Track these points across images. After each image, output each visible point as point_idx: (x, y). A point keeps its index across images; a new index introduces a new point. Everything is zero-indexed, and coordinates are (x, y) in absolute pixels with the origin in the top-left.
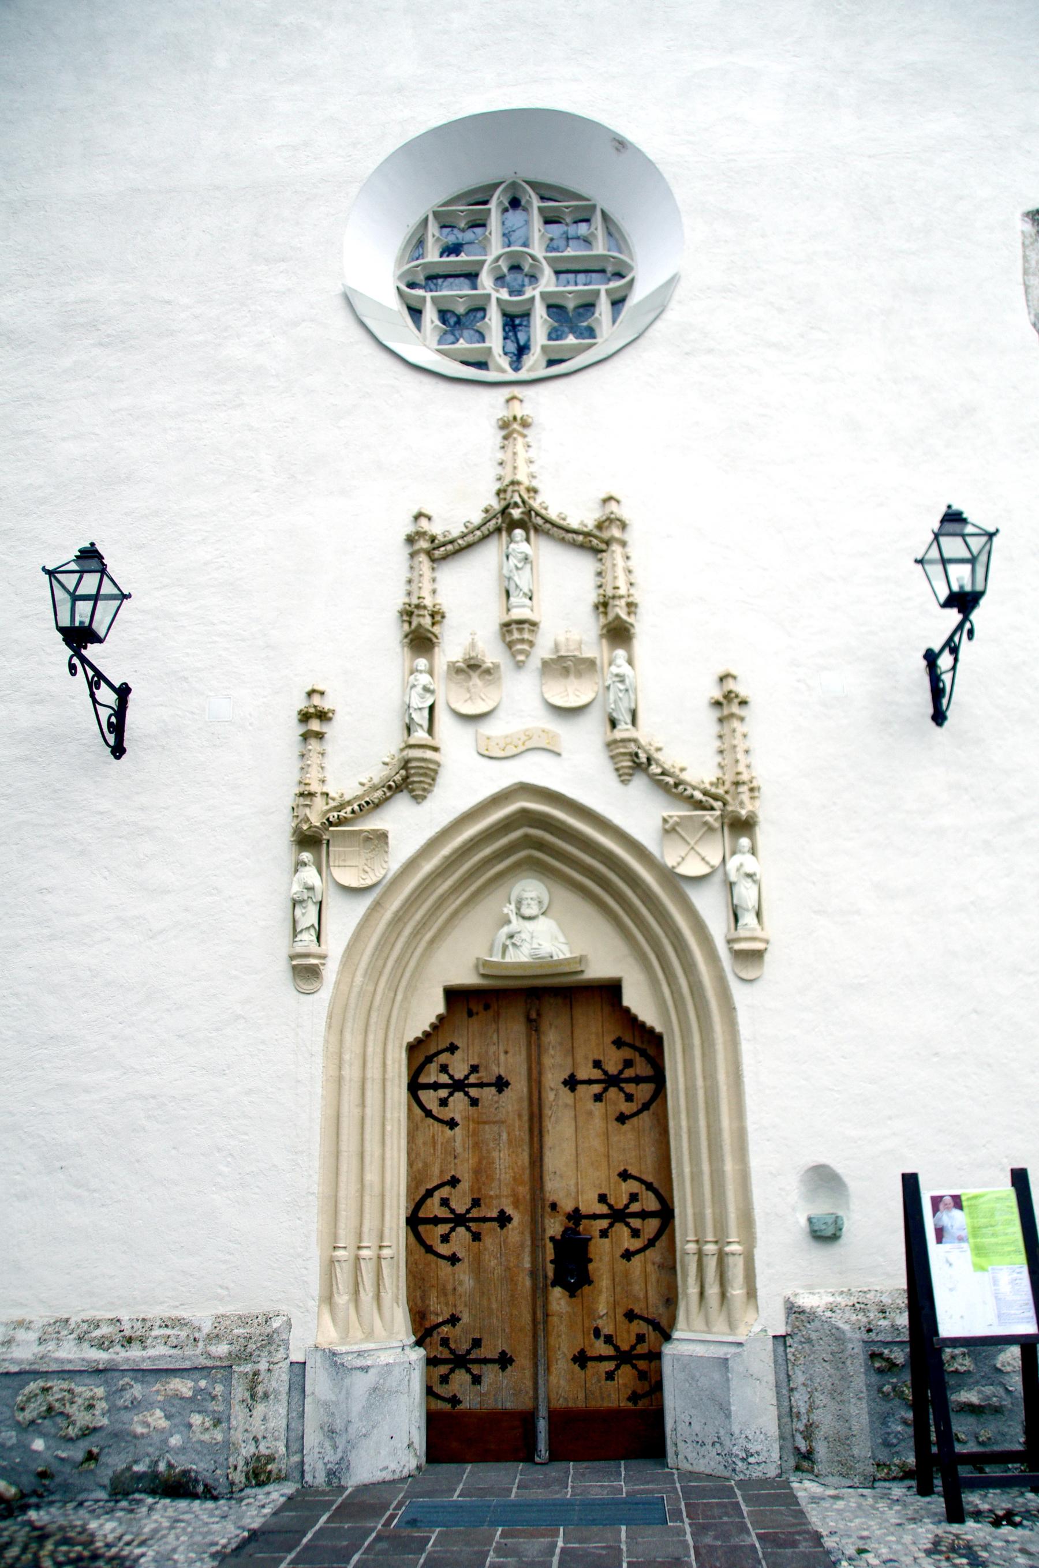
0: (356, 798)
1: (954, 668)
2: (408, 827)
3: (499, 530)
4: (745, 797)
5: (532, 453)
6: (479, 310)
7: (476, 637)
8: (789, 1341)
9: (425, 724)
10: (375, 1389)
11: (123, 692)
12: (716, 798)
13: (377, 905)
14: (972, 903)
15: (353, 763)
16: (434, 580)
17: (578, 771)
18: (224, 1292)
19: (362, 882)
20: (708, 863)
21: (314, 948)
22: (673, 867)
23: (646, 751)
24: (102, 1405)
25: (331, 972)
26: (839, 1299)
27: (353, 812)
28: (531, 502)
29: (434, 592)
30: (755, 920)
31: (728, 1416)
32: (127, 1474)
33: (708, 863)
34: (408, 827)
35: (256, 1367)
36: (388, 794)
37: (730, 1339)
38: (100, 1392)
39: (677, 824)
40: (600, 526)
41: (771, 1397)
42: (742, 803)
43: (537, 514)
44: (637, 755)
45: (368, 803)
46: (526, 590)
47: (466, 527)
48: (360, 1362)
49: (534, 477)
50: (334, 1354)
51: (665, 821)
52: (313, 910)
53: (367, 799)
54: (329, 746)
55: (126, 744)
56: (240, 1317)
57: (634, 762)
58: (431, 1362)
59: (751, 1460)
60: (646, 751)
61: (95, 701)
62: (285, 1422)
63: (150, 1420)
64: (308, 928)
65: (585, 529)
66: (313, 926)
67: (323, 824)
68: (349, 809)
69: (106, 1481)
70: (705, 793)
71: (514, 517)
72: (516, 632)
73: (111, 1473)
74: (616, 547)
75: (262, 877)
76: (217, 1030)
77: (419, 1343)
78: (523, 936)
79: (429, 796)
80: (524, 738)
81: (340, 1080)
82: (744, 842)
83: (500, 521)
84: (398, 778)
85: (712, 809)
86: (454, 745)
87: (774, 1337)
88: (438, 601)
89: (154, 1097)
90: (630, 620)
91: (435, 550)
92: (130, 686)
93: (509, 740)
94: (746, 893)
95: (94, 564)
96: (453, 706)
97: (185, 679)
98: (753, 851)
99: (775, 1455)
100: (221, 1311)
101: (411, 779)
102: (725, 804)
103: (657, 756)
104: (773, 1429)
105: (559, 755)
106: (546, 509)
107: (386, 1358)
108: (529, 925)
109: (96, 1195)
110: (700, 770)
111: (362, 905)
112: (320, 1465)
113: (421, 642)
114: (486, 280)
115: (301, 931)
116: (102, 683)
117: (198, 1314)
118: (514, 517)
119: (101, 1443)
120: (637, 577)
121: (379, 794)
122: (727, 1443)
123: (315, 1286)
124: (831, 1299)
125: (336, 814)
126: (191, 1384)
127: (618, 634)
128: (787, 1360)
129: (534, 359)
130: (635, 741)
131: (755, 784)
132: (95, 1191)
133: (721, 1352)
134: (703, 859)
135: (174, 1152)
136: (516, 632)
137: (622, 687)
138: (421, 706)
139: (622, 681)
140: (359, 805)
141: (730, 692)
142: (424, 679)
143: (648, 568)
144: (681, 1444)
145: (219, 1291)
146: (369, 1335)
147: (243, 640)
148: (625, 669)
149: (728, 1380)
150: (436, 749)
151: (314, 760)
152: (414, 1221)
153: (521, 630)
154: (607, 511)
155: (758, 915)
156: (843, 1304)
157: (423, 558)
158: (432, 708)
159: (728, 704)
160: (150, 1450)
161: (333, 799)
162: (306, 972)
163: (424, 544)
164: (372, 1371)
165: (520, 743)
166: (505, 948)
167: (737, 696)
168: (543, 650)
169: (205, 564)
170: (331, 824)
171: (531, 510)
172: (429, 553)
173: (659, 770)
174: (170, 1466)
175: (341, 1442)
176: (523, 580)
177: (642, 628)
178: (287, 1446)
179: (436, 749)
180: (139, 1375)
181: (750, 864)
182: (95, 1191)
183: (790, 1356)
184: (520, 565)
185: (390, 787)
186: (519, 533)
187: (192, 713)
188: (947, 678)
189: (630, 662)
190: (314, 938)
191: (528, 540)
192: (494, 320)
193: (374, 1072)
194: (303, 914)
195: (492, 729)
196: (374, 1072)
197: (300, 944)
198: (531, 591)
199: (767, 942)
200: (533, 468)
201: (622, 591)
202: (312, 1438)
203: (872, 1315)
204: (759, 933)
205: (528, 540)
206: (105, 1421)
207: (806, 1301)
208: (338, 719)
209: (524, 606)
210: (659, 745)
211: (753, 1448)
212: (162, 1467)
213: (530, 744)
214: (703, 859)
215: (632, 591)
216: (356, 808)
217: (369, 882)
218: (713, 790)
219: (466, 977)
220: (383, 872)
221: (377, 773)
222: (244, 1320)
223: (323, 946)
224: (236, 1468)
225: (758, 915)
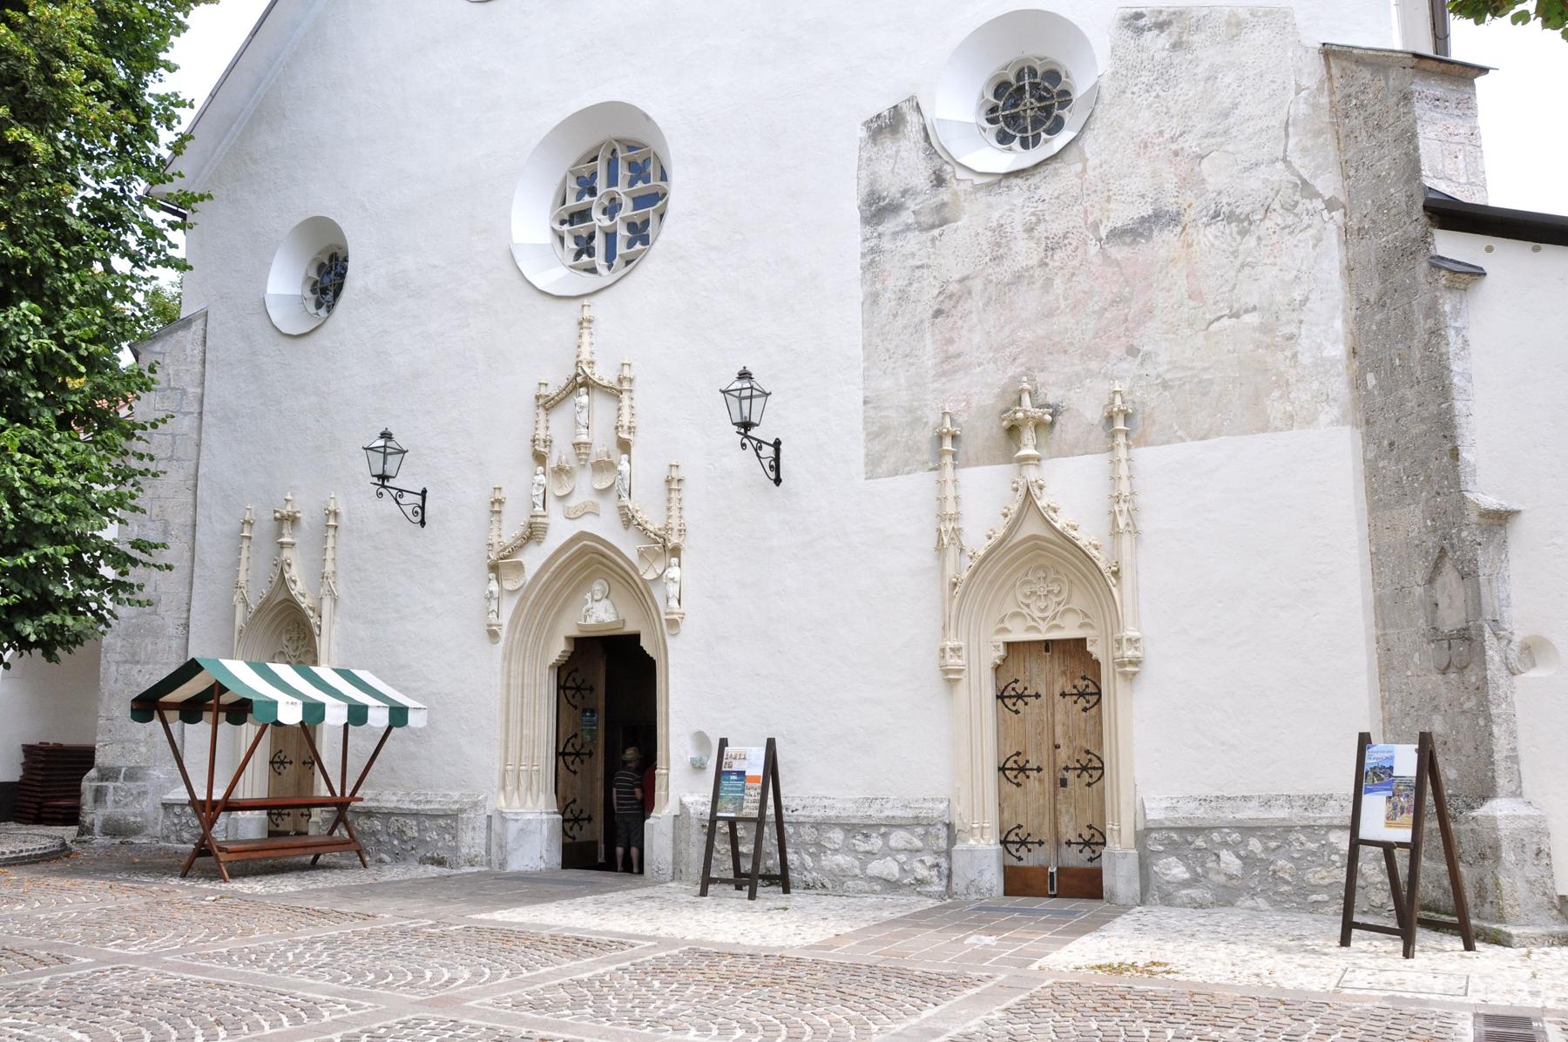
6: (592, 237)
13: (524, 598)
17: (605, 526)
34: (533, 559)
40: (620, 381)
54: (504, 517)
58: (564, 821)
71: (581, 383)
74: (625, 396)
75: (473, 585)
81: (509, 685)
82: (674, 560)
91: (549, 404)
101: (533, 533)
103: (638, 516)
104: (670, 858)
108: (597, 605)
110: (654, 525)
111: (515, 600)
113: (540, 458)
114: (596, 215)
118: (581, 383)
123: (497, 783)
127: (625, 446)
143: (645, 404)
157: (541, 411)
159: (672, 483)
162: (493, 635)
163: (541, 401)
172: (544, 406)
176: (583, 419)
186: (583, 390)
192: (599, 243)
195: (573, 502)
202: (494, 849)
219: (575, 633)
221: (518, 532)
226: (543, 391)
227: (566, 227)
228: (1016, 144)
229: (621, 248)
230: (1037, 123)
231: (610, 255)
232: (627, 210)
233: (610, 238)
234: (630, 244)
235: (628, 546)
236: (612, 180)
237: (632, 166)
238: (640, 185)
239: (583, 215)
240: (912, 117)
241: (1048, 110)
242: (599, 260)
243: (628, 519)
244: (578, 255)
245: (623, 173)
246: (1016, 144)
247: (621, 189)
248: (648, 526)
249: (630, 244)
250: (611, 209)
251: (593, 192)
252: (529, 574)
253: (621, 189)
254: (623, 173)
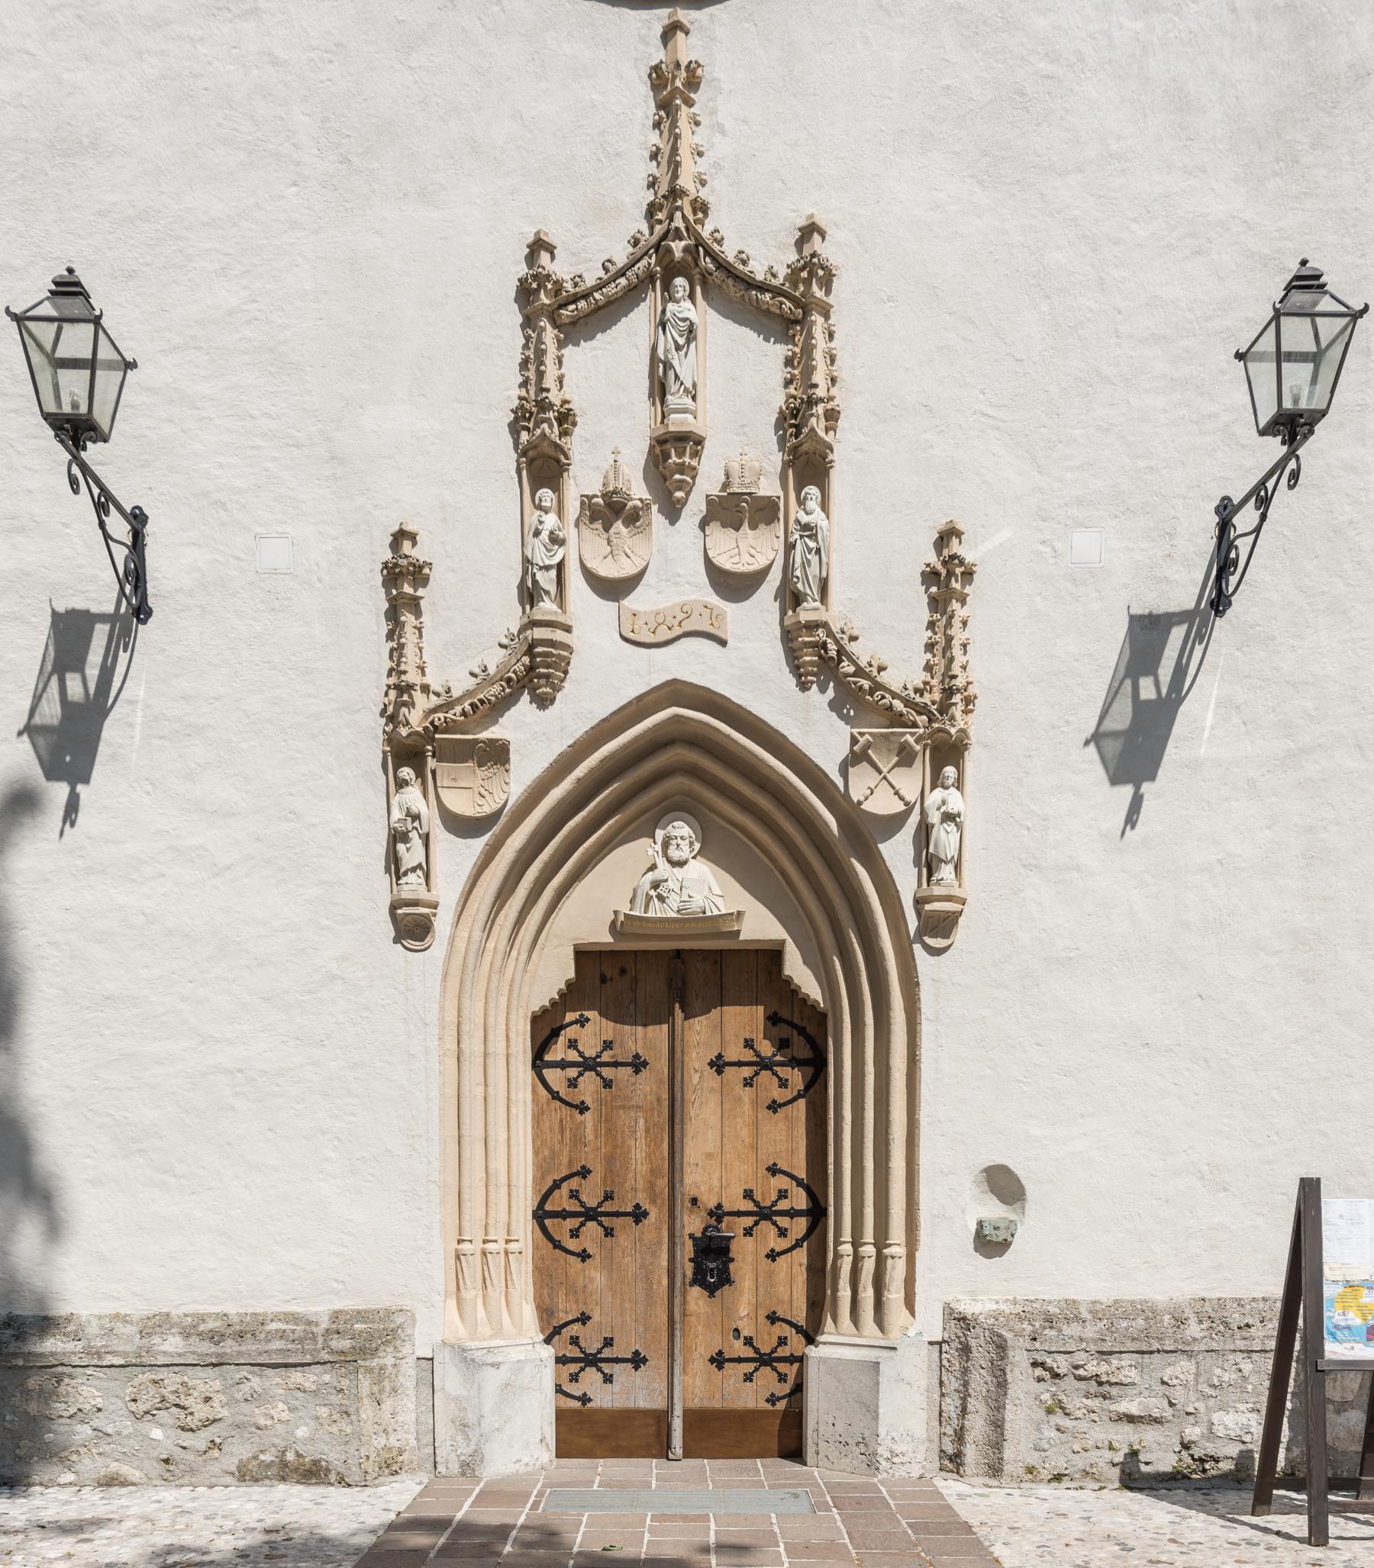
0: (469, 694)
1: (1257, 530)
3: (651, 277)
4: (957, 711)
5: (700, 137)
7: (619, 458)
8: (945, 1347)
9: (552, 588)
10: (507, 1385)
11: (137, 519)
12: (922, 710)
14: (1220, 862)
16: (560, 361)
18: (340, 1286)
19: (479, 809)
20: (902, 798)
21: (422, 894)
22: (860, 803)
23: (837, 642)
24: (218, 1399)
25: (442, 924)
26: (1003, 1307)
27: (464, 713)
28: (699, 227)
29: (560, 380)
30: (953, 875)
31: (876, 1418)
32: (255, 1463)
33: (902, 798)
35: (382, 1361)
36: (508, 690)
37: (883, 1343)
38: (217, 1385)
39: (868, 745)
41: (920, 1400)
42: (952, 718)
43: (709, 252)
44: (824, 646)
45: (482, 702)
46: (689, 385)
47: (606, 270)
48: (491, 1359)
49: (703, 183)
50: (464, 1350)
51: (854, 741)
52: (417, 842)
53: (481, 696)
55: (151, 602)
56: (359, 1312)
57: (820, 657)
59: (895, 1460)
60: (837, 642)
61: (107, 536)
62: (414, 1415)
63: (272, 1412)
64: (413, 870)
65: (775, 282)
66: (420, 866)
67: (426, 729)
68: (458, 709)
69: (233, 1468)
70: (907, 703)
72: (671, 452)
73: (237, 1462)
76: (310, 992)
77: (548, 1341)
78: (670, 884)
79: (559, 696)
80: (680, 616)
83: (653, 261)
84: (519, 667)
85: (915, 725)
87: (931, 1343)
88: (568, 398)
89: (241, 1071)
90: (829, 438)
92: (146, 511)
93: (660, 619)
94: (945, 839)
95: (74, 307)
96: (589, 565)
97: (223, 505)
98: (959, 784)
99: (920, 1457)
100: (338, 1305)
102: (930, 721)
105: (723, 643)
106: (720, 242)
107: (515, 1355)
109: (184, 1181)
112: (453, 1457)
115: (405, 874)
116: (112, 507)
117: (313, 1309)
119: (224, 1434)
120: (842, 369)
121: (496, 689)
122: (872, 1445)
124: (995, 1307)
125: (441, 715)
126: (312, 1378)
128: (941, 1366)
130: (825, 625)
131: (971, 690)
132: (183, 1176)
133: (870, 1355)
134: (897, 793)
135: (270, 1134)
136: (671, 452)
137: (812, 544)
138: (547, 562)
139: (814, 537)
140: (471, 705)
141: (953, 557)
142: (551, 521)
144: (822, 1445)
145: (335, 1285)
146: (499, 1332)
147: (297, 446)
148: (817, 517)
149: (877, 1383)
150: (568, 629)
151: (410, 637)
152: (540, 1215)
153: (680, 455)
154: (807, 252)
155: (957, 868)
156: (1007, 1311)
158: (560, 567)
160: (276, 1441)
161: (438, 695)
164: (503, 1368)
165: (676, 623)
166: (649, 898)
167: (962, 563)
168: (708, 482)
169: (231, 313)
170: (436, 729)
171: (699, 242)
173: (852, 669)
174: (298, 1455)
175: (474, 1436)
177: (847, 449)
178: (417, 1439)
179: (568, 629)
180: (256, 1369)
181: (955, 801)
182: (183, 1176)
183: (945, 1362)
184: (681, 341)
185: (509, 680)
187: (238, 558)
188: (1243, 545)
189: (825, 506)
190: (422, 881)
191: (692, 297)
193: (498, 1045)
194: (408, 849)
196: (498, 1045)
197: (405, 887)
198: (694, 386)
199: (963, 902)
200: (703, 165)
201: (820, 392)
203: (1037, 1324)
204: (957, 892)
205: (692, 297)
206: (224, 1413)
207: (967, 1308)
208: (436, 576)
209: (685, 411)
210: (855, 633)
211: (898, 1449)
212: (290, 1456)
213: (688, 626)
214: (897, 793)
215: (834, 391)
216: (468, 708)
217: (488, 809)
218: (918, 699)
220: (504, 797)
222: (361, 1315)
223: (434, 892)
224: (368, 1457)
225: (957, 868)
248: (884, 678)
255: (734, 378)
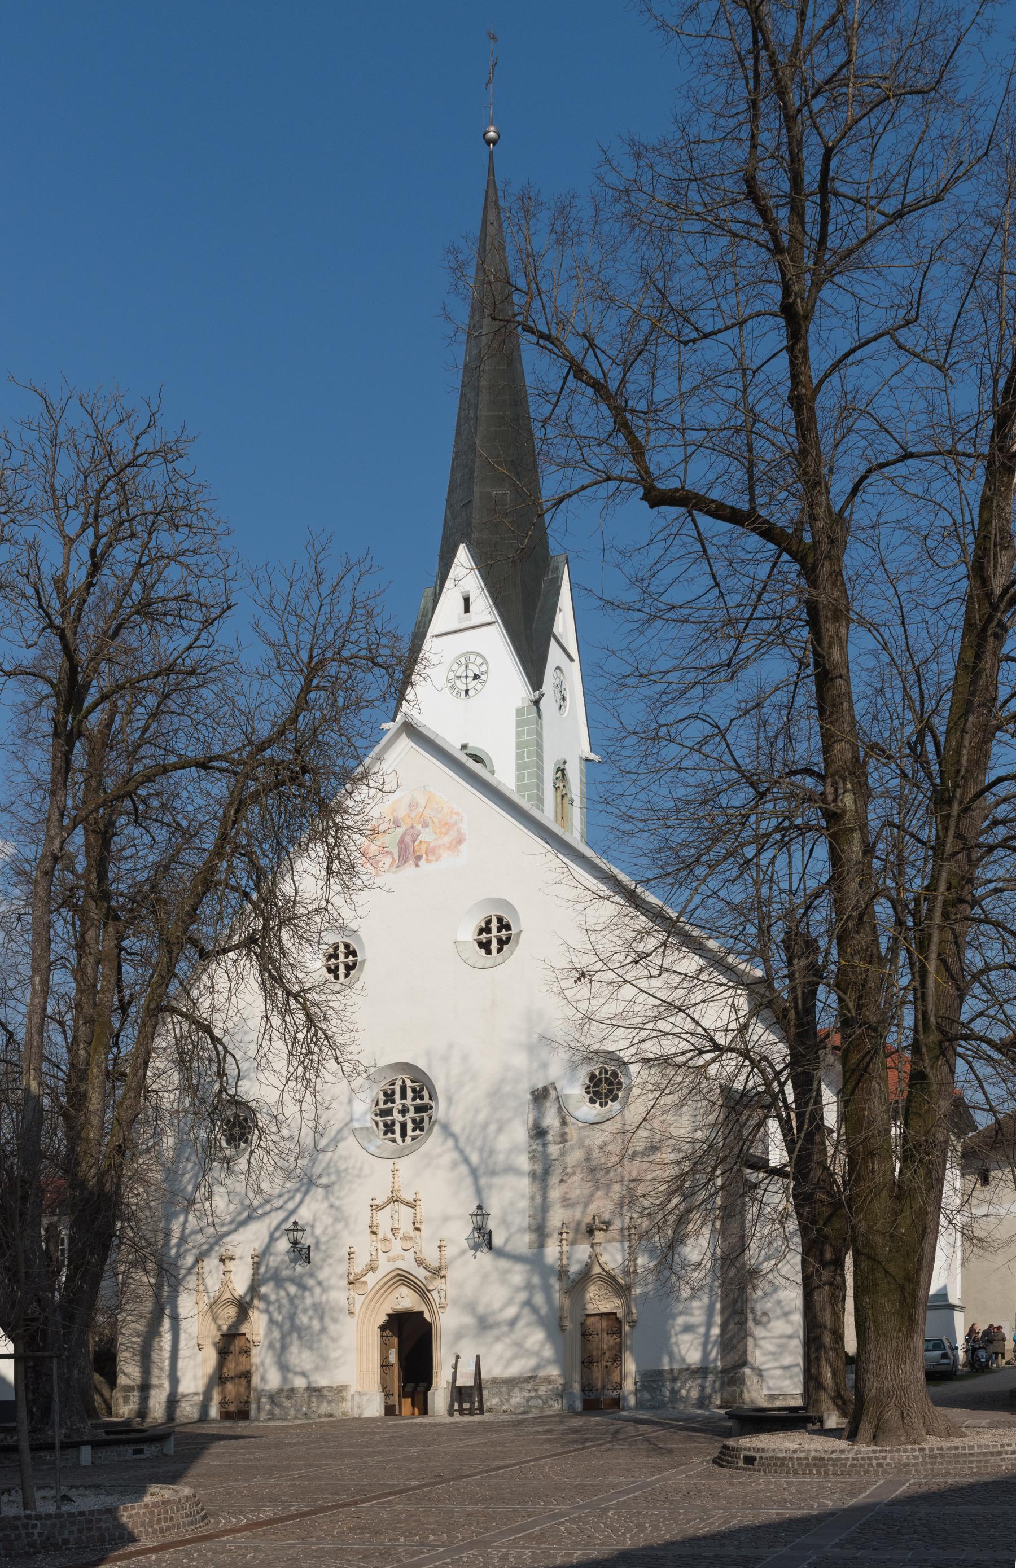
2: (371, 1279)
6: (393, 1123)
15: (360, 1264)
17: (408, 1264)
34: (371, 1279)
86: (382, 1258)
91: (376, 1208)
101: (372, 1268)
114: (395, 1113)
129: (408, 1139)
181: (443, 1287)
192: (397, 1128)
226: (376, 1202)
227: (378, 1118)
228: (597, 1105)
229: (409, 1132)
230: (607, 1096)
231: (404, 1134)
232: (412, 1113)
233: (404, 1126)
234: (414, 1130)
235: (421, 1273)
236: (404, 1096)
237: (414, 1090)
238: (418, 1101)
239: (388, 1112)
240: (553, 1093)
241: (611, 1091)
242: (397, 1135)
243: (420, 1262)
244: (385, 1133)
245: (410, 1094)
246: (597, 1105)
247: (408, 1102)
249: (414, 1130)
250: (404, 1111)
251: (393, 1101)
252: (370, 1286)
253: (408, 1102)
254: (410, 1094)
255: (405, 1213)
